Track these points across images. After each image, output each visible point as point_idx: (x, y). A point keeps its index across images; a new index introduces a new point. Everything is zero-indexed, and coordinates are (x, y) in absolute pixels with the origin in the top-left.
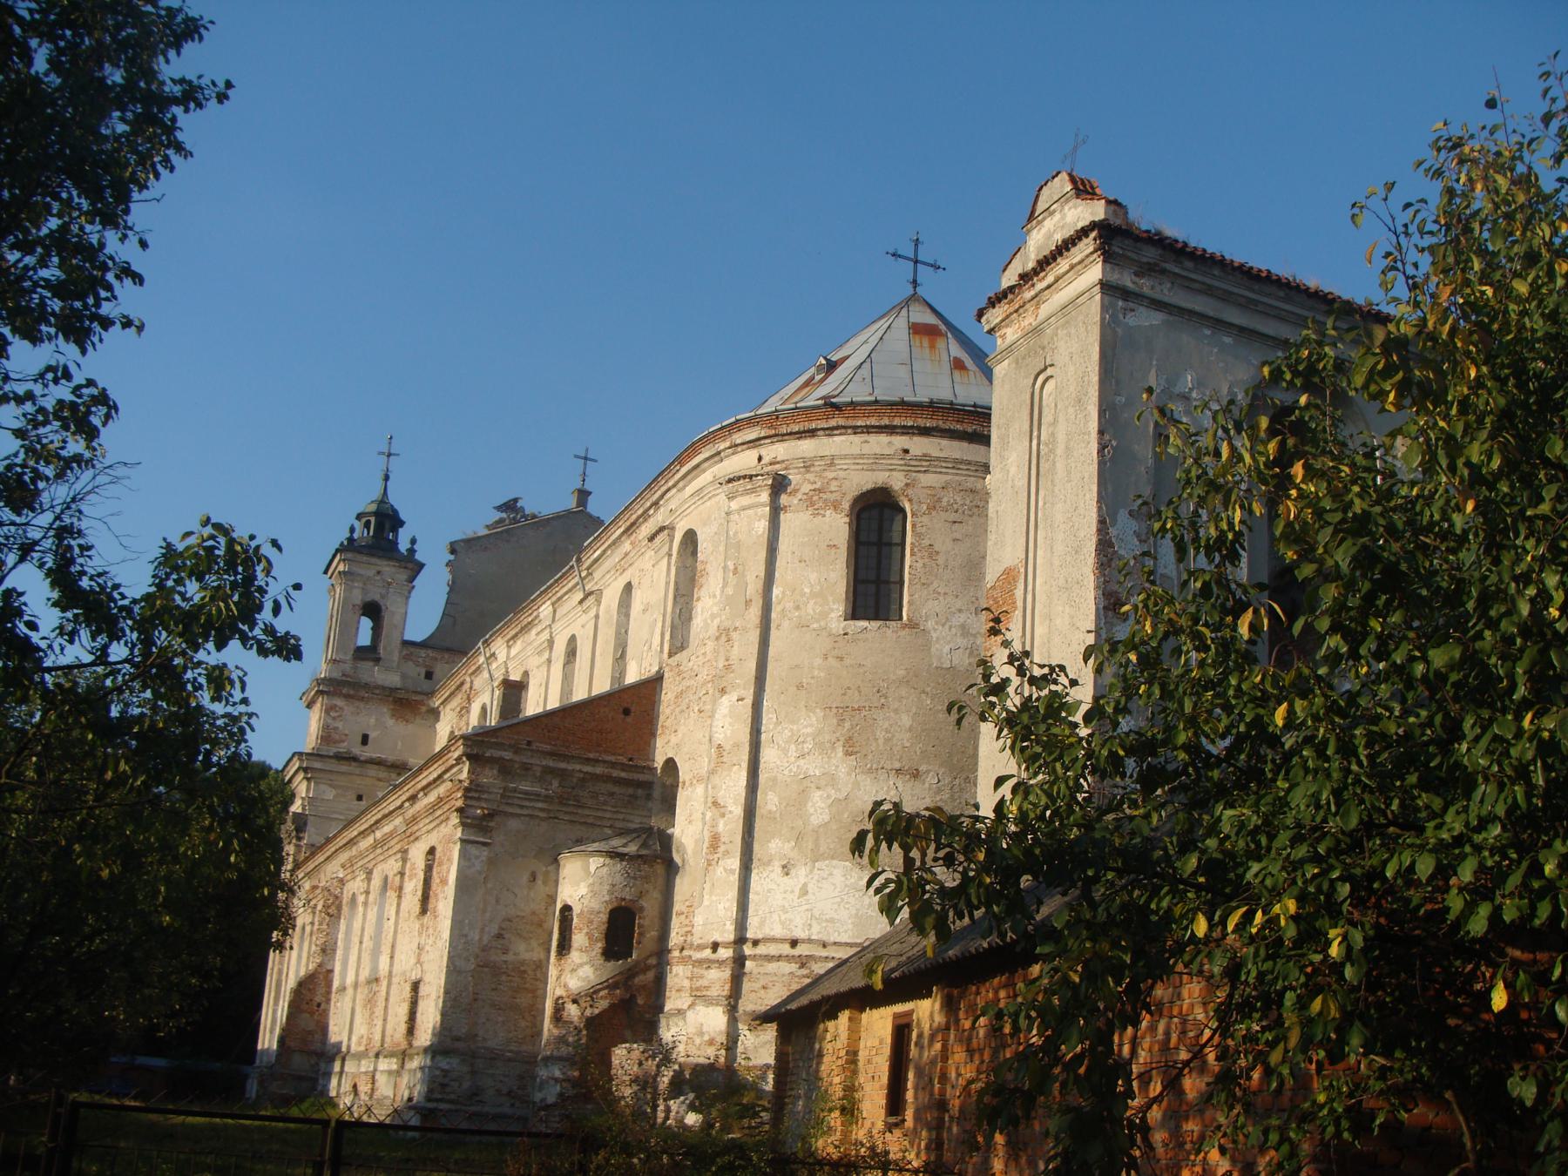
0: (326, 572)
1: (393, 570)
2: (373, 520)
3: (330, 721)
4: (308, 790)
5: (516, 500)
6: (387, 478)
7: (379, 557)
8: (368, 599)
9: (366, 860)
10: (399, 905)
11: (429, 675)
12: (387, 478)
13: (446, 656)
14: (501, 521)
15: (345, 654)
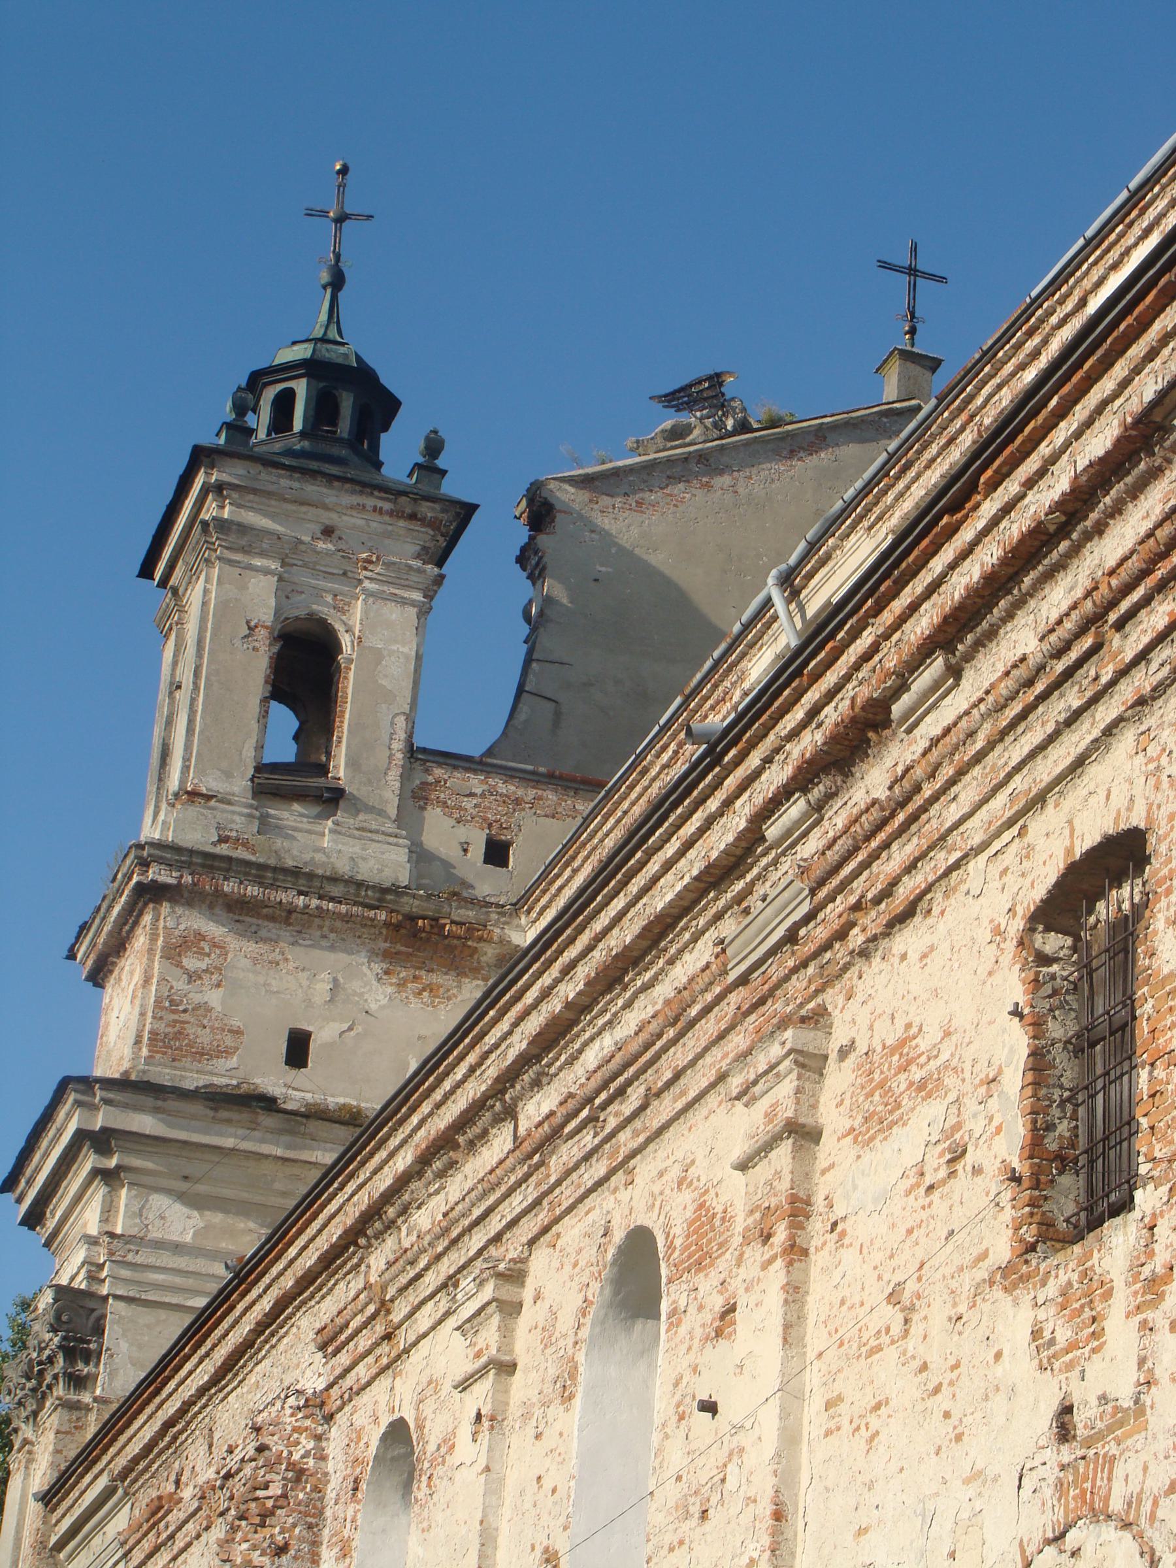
0: (146, 571)
1: (376, 524)
2: (301, 387)
3: (180, 984)
4: (108, 1212)
5: (716, 379)
6: (337, 282)
7: (331, 479)
8: (298, 609)
9: (476, 1241)
10: (795, 1292)
11: (497, 853)
12: (337, 282)
13: (551, 796)
14: (677, 433)
15: (228, 775)
